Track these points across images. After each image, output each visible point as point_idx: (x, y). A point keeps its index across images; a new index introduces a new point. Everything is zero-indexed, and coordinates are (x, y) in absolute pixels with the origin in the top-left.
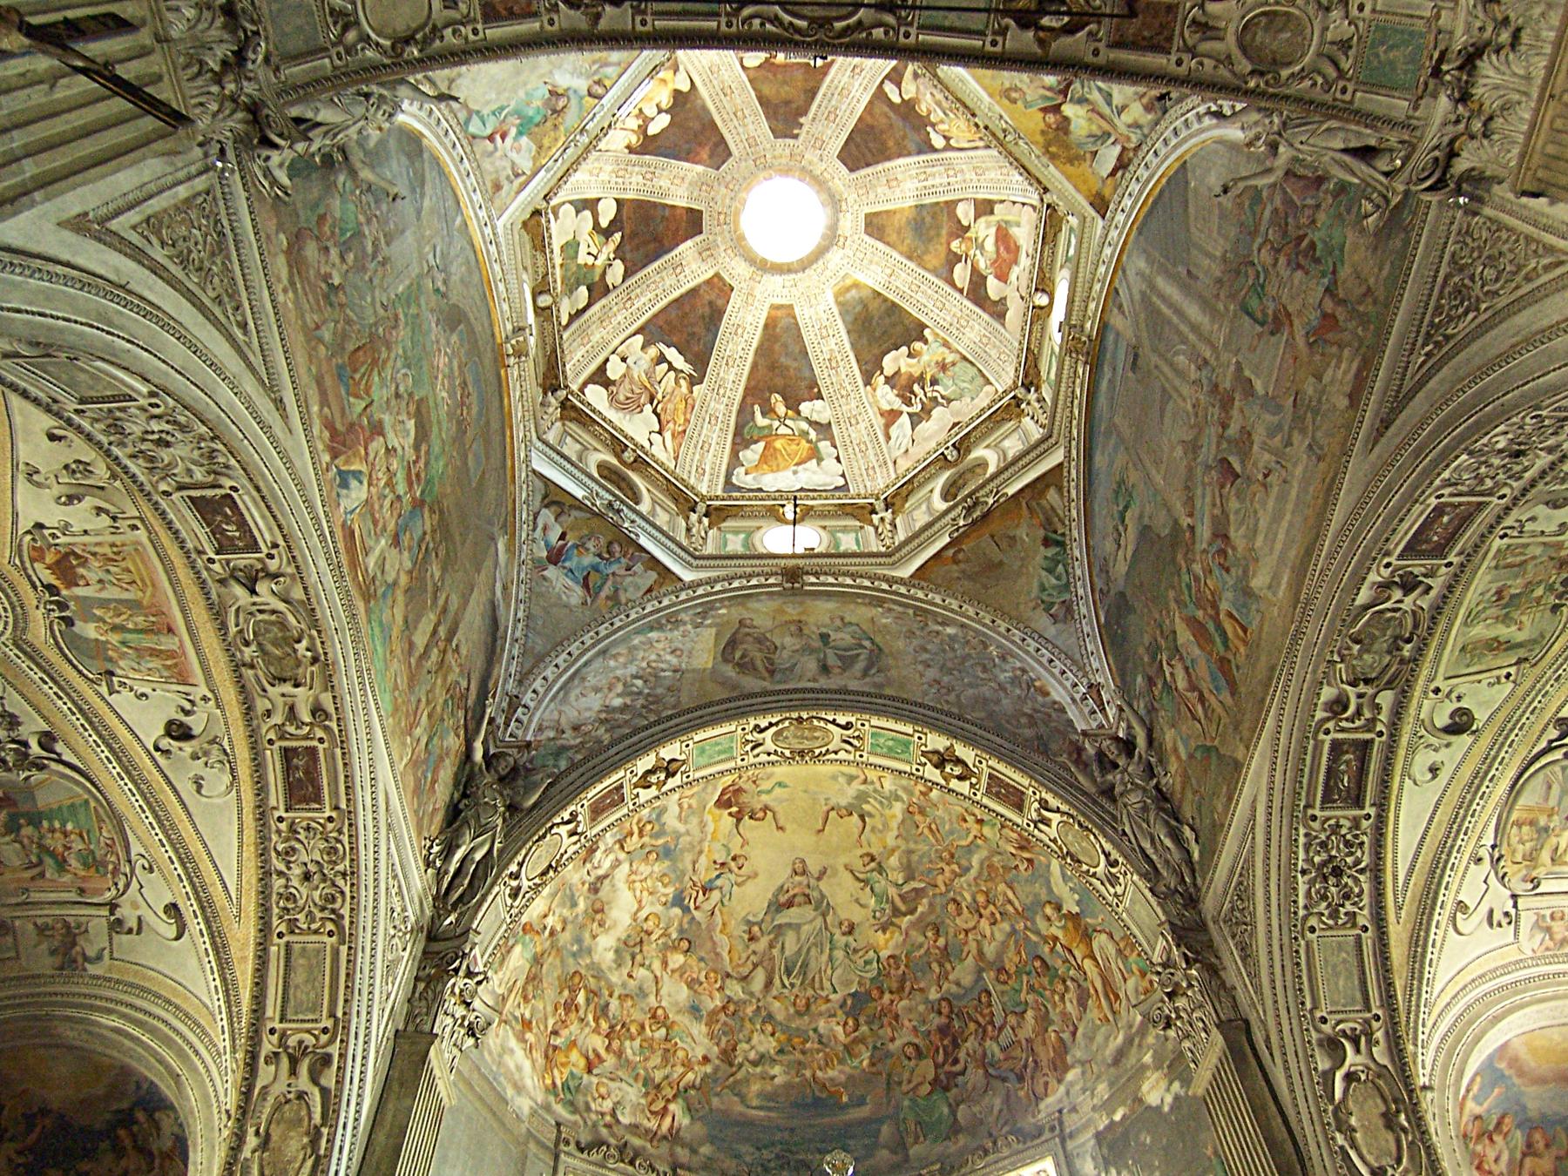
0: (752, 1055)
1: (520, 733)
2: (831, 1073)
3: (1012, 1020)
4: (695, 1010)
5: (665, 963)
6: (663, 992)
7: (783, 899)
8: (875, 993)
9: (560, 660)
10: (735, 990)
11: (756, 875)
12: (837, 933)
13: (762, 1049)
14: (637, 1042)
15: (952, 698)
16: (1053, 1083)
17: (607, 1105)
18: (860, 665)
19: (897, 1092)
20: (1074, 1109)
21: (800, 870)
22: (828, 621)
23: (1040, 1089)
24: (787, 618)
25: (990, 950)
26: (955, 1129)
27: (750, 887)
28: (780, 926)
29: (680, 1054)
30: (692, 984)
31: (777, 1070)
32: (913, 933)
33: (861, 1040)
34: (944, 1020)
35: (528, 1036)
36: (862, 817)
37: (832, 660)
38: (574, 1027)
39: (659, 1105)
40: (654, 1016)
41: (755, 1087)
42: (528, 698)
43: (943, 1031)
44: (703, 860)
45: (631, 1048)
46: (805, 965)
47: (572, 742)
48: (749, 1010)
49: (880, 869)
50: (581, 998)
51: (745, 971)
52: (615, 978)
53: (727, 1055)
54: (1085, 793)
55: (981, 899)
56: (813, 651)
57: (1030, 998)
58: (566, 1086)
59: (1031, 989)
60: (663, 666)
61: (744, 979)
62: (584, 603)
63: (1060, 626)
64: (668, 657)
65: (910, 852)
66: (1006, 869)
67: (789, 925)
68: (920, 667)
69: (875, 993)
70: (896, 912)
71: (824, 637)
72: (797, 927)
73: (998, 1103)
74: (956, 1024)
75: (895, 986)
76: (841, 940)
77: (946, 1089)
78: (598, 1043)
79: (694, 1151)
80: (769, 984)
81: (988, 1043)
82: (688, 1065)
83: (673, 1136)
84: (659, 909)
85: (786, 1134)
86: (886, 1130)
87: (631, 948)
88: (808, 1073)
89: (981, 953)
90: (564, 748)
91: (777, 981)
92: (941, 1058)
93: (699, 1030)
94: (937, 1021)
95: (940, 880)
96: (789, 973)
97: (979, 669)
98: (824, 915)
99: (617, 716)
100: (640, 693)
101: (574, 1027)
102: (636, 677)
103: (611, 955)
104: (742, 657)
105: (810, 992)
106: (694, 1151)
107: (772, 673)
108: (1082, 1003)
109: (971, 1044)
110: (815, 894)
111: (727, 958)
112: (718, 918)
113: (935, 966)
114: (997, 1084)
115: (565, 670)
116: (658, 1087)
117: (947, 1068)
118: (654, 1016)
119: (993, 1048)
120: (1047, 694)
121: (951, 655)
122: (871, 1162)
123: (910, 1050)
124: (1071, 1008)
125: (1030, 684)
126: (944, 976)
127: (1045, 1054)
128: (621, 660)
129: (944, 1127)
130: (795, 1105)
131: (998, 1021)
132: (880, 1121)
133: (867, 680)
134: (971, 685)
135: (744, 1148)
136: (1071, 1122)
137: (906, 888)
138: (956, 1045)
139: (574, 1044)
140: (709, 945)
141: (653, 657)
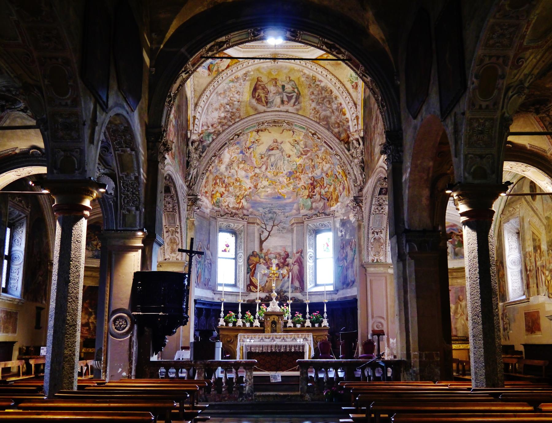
0: (262, 186)
1: (197, 129)
2: (282, 190)
3: (328, 186)
4: (247, 177)
5: (238, 167)
6: (238, 174)
7: (271, 148)
8: (295, 172)
9: (204, 99)
10: (257, 171)
11: (263, 143)
12: (286, 157)
13: (265, 185)
14: (232, 187)
15: (318, 116)
16: (335, 204)
17: (226, 204)
18: (293, 101)
19: (299, 196)
20: (337, 212)
21: (276, 141)
22: (284, 79)
23: (332, 204)
24: (272, 77)
25: (325, 169)
26: (311, 208)
27: (262, 146)
28: (270, 155)
29: (244, 188)
30: (246, 171)
31: (268, 190)
32: (306, 160)
33: (291, 183)
34: (311, 182)
35: (207, 195)
36: (293, 132)
37: (285, 99)
38: (217, 188)
39: (239, 201)
40: (236, 180)
41: (263, 194)
42: (198, 116)
43: (312, 184)
44: (248, 142)
45: (231, 189)
46: (276, 164)
47: (212, 131)
48: (261, 175)
49: (298, 144)
50: (218, 181)
51: (260, 166)
52: (226, 174)
53: (256, 187)
54: (346, 154)
55: (324, 157)
56: (280, 93)
57: (333, 183)
58: (217, 202)
59: (333, 181)
60: (235, 99)
61: (260, 168)
62: (209, 75)
63: (354, 90)
64: (236, 95)
65: (306, 142)
66: (330, 154)
67: (272, 155)
68: (311, 102)
69: (295, 172)
70: (302, 154)
71: (283, 87)
72: (275, 155)
73: (321, 204)
74: (315, 183)
75: (300, 171)
76: (286, 158)
77: (311, 198)
78: (223, 190)
79: (248, 211)
80: (266, 169)
81: (322, 190)
82: (245, 190)
83: (243, 208)
84: (236, 155)
85: (270, 205)
86: (295, 206)
87: (230, 166)
88: (277, 190)
89: (322, 169)
90: (210, 134)
91: (269, 168)
92: (310, 190)
93: (248, 181)
94: (310, 182)
95: (314, 150)
96: (272, 166)
97: (328, 103)
98: (282, 152)
99: (223, 121)
100: (228, 111)
101: (217, 188)
102: (227, 104)
103: (225, 169)
104: (258, 96)
105: (278, 171)
106: (248, 211)
107: (267, 103)
108: (344, 188)
109: (318, 189)
110: (279, 147)
111: (255, 163)
112: (253, 154)
113: (311, 169)
114: (322, 200)
115: (207, 102)
116: (238, 197)
117: (312, 193)
118: (236, 180)
119: (323, 192)
120: (345, 114)
121: (320, 96)
122: (290, 213)
123: (303, 187)
124: (341, 189)
125: (341, 111)
126: (313, 171)
127: (334, 197)
128: (222, 96)
129: (309, 207)
130: (273, 198)
131: (325, 185)
132: (294, 203)
133: (295, 107)
134: (325, 110)
135: (260, 209)
136: (336, 214)
137: (305, 149)
138: (314, 188)
139: (217, 192)
140: (250, 161)
141: (231, 95)
